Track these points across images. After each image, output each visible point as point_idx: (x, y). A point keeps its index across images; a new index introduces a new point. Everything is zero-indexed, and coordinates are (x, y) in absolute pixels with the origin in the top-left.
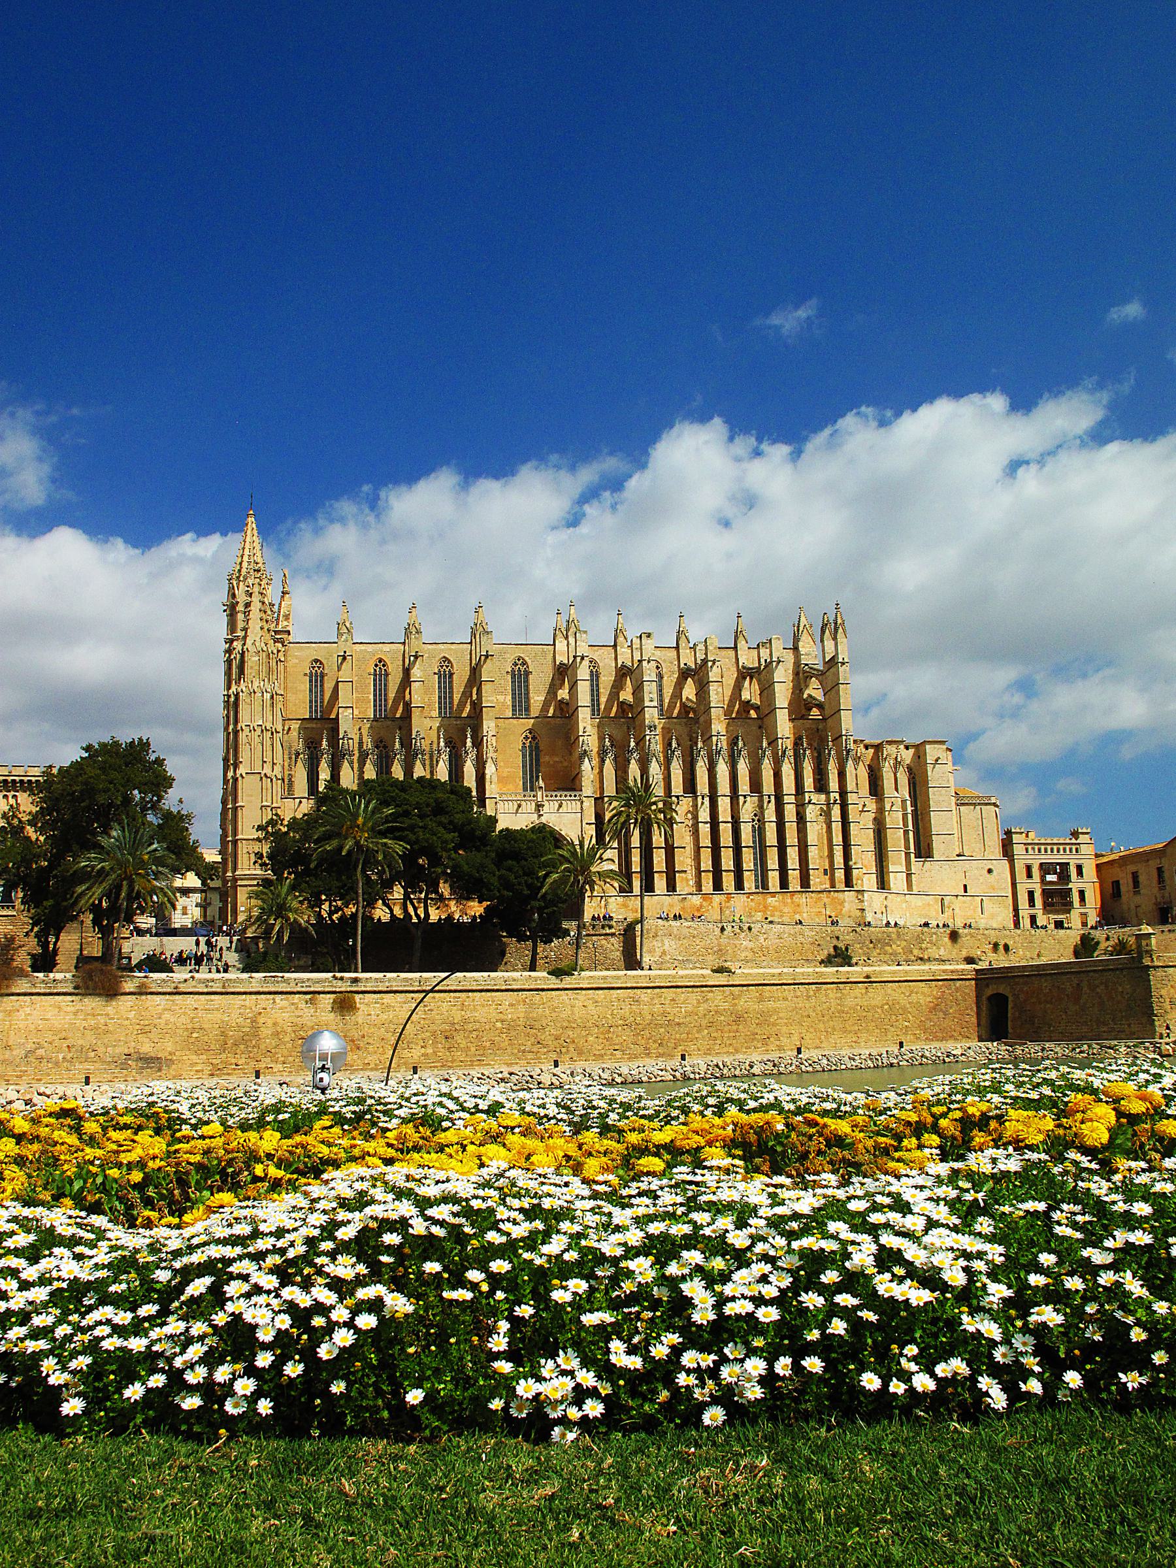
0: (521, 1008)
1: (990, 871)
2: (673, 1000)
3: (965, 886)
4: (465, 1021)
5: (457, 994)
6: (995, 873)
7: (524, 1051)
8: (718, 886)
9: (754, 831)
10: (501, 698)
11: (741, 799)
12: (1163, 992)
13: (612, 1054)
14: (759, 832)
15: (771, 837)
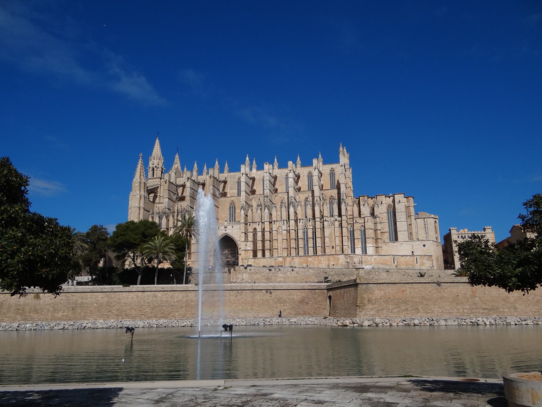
0: (106, 298)
1: (424, 246)
2: (172, 296)
3: (413, 252)
4: (82, 303)
5: (81, 294)
6: (426, 246)
7: (103, 315)
8: (289, 254)
9: (304, 232)
10: (233, 191)
11: (299, 221)
12: (364, 296)
13: (140, 317)
14: (305, 233)
15: (310, 235)
